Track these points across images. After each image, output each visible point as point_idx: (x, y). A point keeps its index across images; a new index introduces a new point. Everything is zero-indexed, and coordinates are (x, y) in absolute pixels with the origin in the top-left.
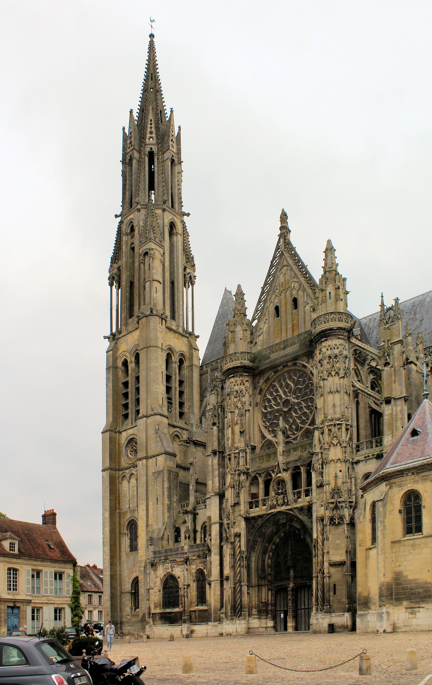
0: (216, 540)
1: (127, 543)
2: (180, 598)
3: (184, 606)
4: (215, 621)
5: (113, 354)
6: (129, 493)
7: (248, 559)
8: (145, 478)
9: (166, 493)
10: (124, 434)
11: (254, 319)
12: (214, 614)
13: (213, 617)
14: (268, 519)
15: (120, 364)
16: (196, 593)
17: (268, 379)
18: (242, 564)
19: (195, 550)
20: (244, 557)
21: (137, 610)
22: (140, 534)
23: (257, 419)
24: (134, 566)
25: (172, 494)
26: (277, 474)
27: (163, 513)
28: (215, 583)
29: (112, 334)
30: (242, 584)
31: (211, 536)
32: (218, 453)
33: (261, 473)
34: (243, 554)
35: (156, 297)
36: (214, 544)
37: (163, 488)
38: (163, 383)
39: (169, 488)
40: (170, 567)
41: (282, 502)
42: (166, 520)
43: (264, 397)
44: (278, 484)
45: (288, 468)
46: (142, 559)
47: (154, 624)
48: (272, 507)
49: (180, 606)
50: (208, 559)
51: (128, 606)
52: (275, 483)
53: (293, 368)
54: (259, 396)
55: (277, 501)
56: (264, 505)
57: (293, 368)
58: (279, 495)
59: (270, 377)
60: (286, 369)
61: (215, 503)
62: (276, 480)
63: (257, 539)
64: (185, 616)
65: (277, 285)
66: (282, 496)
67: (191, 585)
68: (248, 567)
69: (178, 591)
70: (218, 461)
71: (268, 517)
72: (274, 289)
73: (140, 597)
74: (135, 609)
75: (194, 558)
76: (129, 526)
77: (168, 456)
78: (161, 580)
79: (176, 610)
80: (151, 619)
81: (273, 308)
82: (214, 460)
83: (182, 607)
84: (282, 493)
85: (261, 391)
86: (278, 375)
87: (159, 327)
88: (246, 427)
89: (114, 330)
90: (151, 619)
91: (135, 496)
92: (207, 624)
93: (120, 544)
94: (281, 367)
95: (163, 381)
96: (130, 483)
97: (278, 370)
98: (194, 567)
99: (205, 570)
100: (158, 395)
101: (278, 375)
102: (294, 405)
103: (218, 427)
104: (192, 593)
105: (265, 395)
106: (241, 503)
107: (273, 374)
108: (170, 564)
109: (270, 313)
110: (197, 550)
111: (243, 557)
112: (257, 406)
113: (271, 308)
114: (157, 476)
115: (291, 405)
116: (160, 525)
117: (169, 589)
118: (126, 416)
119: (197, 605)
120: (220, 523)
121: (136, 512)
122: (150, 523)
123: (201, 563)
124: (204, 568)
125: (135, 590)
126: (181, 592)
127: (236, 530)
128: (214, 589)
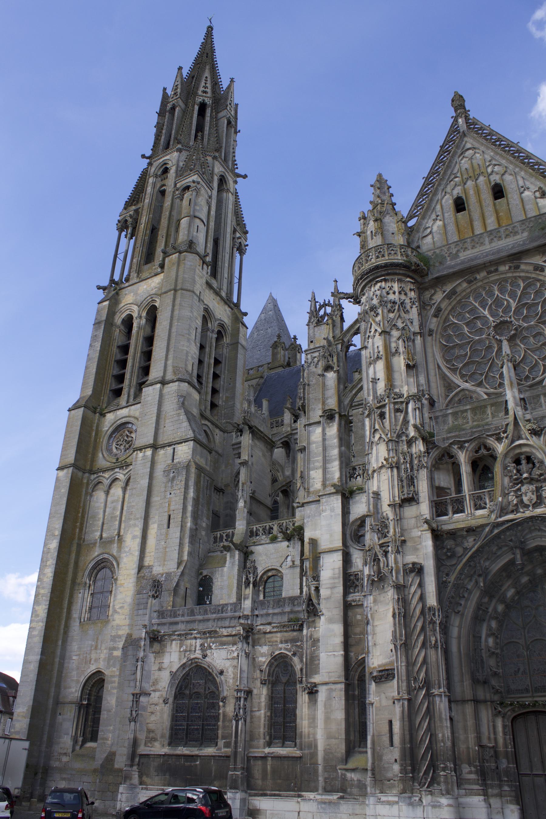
0: (332, 588)
1: (85, 603)
2: (220, 723)
3: (236, 742)
4: (327, 790)
5: (109, 304)
6: (105, 511)
7: (445, 629)
8: (147, 481)
9: (190, 508)
10: (110, 417)
11: (410, 217)
12: (325, 769)
13: (321, 779)
14: (498, 536)
15: (118, 320)
16: (269, 714)
17: (453, 292)
18: (433, 639)
19: (271, 611)
20: (438, 622)
21: (89, 745)
22: (122, 582)
23: (434, 356)
24: (96, 648)
25: (200, 513)
26: (513, 442)
27: (181, 545)
28: (331, 690)
29: (112, 281)
30: (435, 691)
31: (318, 581)
32: (337, 416)
33: (465, 442)
34: (434, 615)
35: (197, 236)
36: (328, 599)
37: (185, 498)
38: (195, 343)
39: (196, 501)
40: (198, 647)
41: (534, 497)
42: (185, 558)
43: (445, 322)
44: (517, 462)
45: (542, 430)
46: (120, 633)
47: (141, 783)
48: (503, 511)
49: (221, 743)
50: (305, 632)
51: (67, 734)
52: (508, 460)
53: (510, 275)
54: (435, 320)
55: (519, 497)
56: (478, 507)
57: (510, 275)
58: (522, 483)
59: (459, 289)
60: (494, 277)
61: (332, 510)
62: (511, 454)
63: (466, 582)
64: (235, 769)
65: (455, 171)
66: (532, 487)
67: (255, 691)
68: (446, 652)
69: (215, 706)
70: (339, 430)
71: (496, 531)
72: (449, 178)
73: (104, 715)
74: (84, 742)
75: (268, 628)
76: (96, 571)
77: (198, 446)
78: (173, 675)
79: (210, 751)
80: (135, 768)
81: (451, 202)
82: (327, 430)
83: (227, 745)
84: (531, 480)
85: (439, 310)
86: (475, 287)
87: (199, 270)
88: (419, 358)
89: (116, 278)
90: (135, 768)
91: (116, 517)
92: (299, 796)
93: (70, 603)
94: (483, 274)
95: (197, 341)
96: (109, 496)
97: (476, 279)
98: (264, 649)
99: (296, 659)
100: (187, 356)
101: (475, 287)
102: (522, 330)
103: (338, 372)
104: (257, 714)
105: (446, 319)
106: (421, 500)
107: (465, 285)
108: (199, 642)
109: (445, 207)
110: (276, 611)
111: (432, 622)
112: (430, 335)
113: (447, 201)
114: (174, 478)
115: (516, 329)
116: (171, 566)
117: (191, 698)
118: (118, 393)
119: (269, 744)
120: (343, 550)
121: (115, 545)
122: (146, 564)
123: (286, 642)
124: (294, 654)
125: (89, 700)
126: (229, 709)
127: (410, 558)
128: (327, 705)
